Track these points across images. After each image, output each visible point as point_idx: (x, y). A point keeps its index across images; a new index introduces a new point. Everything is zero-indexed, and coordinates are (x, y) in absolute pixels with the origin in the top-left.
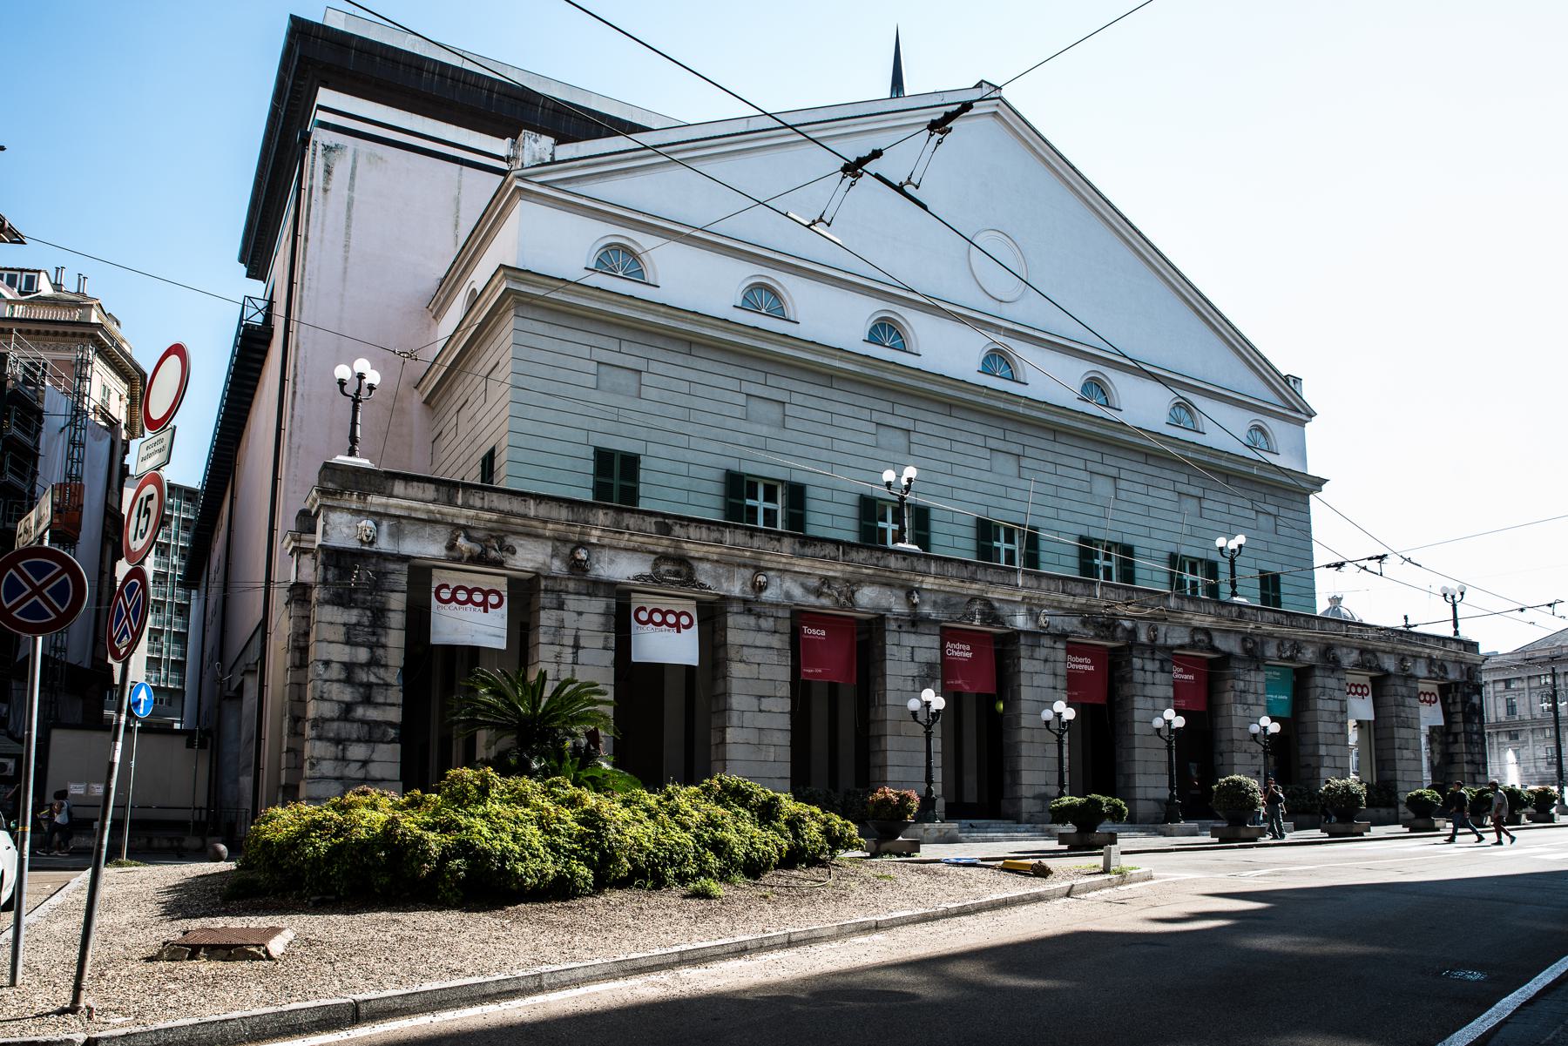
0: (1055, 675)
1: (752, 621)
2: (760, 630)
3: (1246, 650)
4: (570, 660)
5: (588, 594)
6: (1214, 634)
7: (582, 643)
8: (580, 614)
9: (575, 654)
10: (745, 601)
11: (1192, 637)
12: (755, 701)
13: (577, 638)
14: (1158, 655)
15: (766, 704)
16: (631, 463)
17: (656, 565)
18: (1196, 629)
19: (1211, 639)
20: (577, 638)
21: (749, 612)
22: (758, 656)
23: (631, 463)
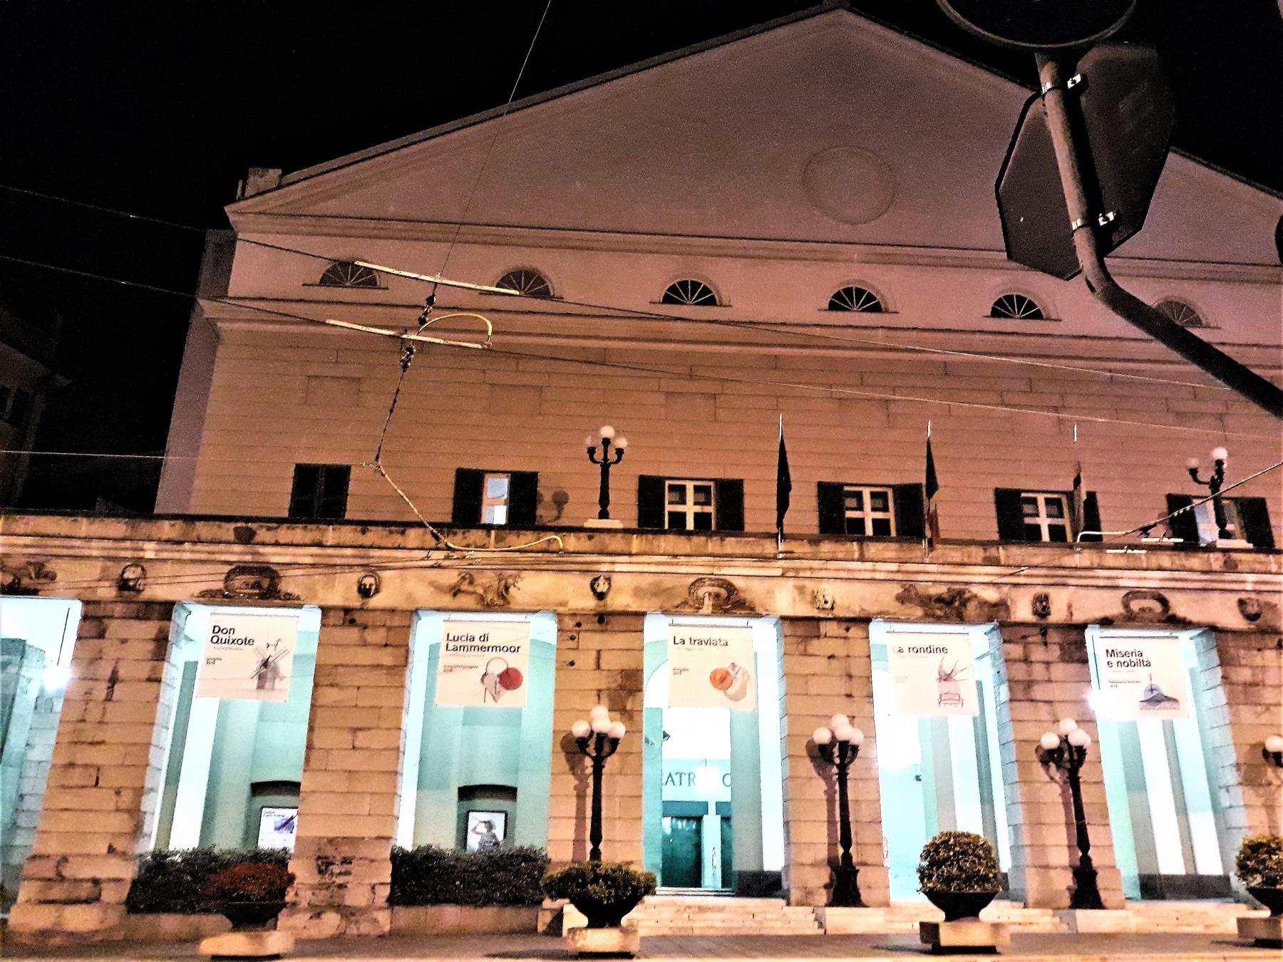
0: (850, 676)
1: (354, 633)
2: (365, 644)
3: (1252, 618)
4: (103, 695)
5: (138, 618)
6: (1173, 598)
7: (122, 673)
8: (124, 641)
9: (111, 688)
10: (347, 611)
11: (1126, 606)
12: (349, 737)
13: (115, 672)
14: (1054, 637)
15: (362, 740)
16: (339, 475)
17: (228, 577)
18: (1133, 594)
19: (1164, 602)
20: (115, 672)
21: (352, 622)
22: (360, 678)
23: (339, 475)
